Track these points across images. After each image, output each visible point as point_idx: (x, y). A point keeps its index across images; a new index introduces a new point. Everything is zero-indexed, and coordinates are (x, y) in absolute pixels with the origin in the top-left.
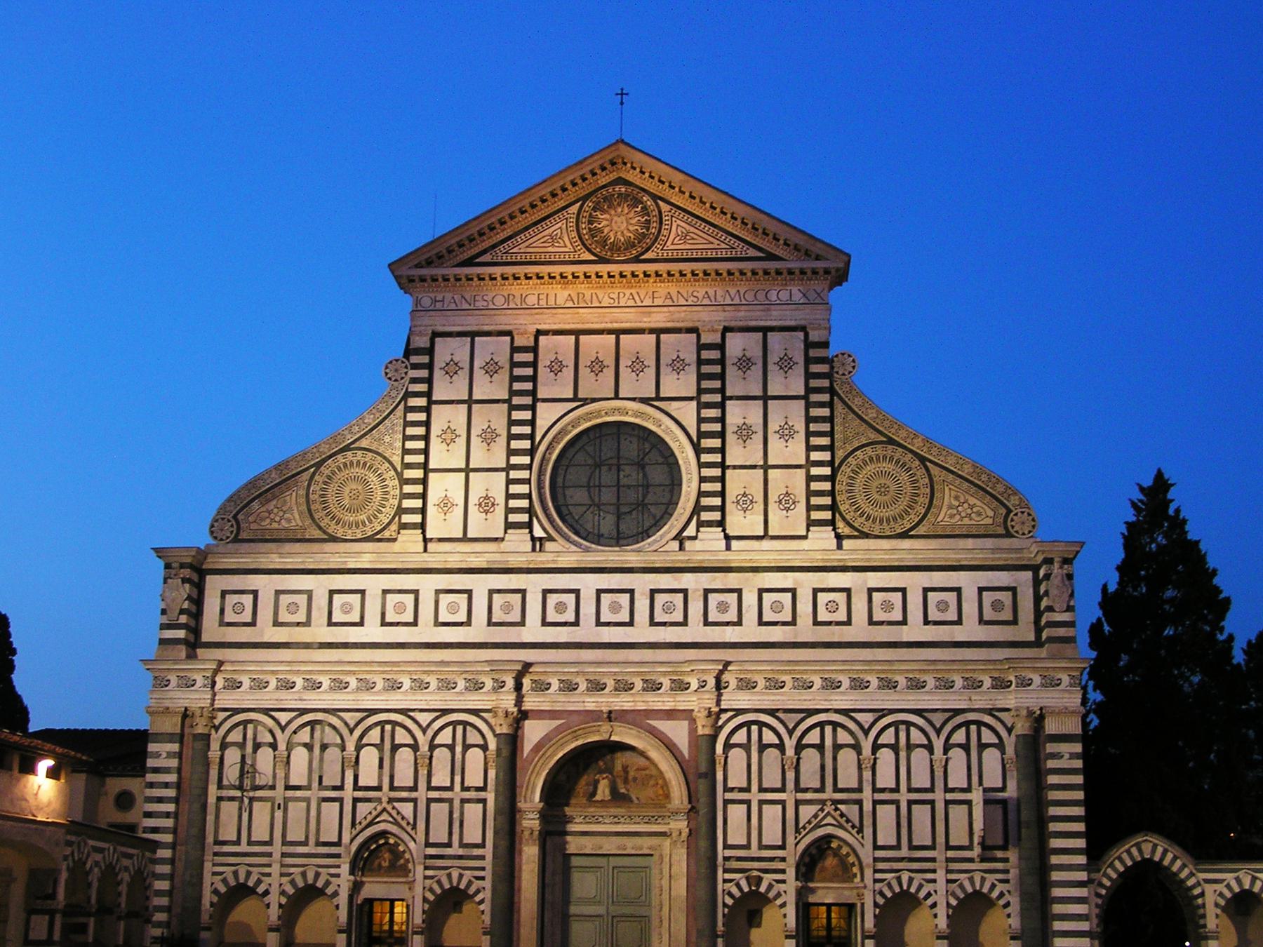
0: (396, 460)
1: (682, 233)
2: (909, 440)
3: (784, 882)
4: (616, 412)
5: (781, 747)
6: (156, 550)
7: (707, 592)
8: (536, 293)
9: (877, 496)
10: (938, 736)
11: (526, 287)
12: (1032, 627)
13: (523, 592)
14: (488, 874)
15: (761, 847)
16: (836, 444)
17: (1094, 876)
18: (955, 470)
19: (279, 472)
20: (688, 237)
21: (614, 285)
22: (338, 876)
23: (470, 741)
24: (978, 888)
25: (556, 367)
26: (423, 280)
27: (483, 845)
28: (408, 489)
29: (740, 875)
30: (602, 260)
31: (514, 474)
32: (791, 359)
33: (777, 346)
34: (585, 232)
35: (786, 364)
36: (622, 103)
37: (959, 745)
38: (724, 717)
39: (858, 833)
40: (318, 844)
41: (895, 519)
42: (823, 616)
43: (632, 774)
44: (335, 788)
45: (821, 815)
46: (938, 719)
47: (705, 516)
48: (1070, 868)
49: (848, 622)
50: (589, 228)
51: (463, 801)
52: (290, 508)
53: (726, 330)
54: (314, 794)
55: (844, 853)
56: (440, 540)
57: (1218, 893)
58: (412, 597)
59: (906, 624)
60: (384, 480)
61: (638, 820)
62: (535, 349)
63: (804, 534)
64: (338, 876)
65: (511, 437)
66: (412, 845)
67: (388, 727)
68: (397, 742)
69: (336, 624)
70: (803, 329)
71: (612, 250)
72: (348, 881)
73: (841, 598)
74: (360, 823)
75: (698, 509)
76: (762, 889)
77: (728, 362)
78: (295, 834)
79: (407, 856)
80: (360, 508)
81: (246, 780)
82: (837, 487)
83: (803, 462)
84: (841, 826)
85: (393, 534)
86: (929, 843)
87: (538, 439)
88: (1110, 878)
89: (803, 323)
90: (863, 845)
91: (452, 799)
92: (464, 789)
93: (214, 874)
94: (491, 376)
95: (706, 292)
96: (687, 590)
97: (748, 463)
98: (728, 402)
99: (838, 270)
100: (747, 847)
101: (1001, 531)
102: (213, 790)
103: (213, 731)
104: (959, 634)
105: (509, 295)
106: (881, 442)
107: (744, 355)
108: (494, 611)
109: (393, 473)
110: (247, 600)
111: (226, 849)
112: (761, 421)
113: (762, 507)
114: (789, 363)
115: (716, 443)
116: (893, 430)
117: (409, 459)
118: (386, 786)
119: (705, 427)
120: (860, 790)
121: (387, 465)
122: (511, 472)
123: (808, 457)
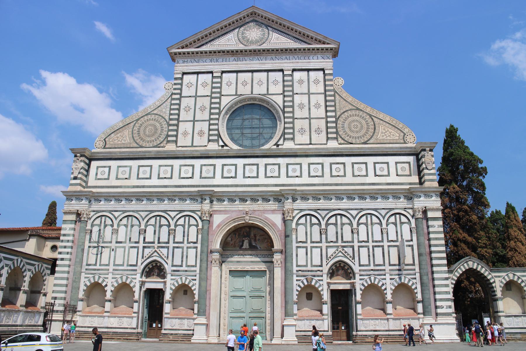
0: (167, 118)
3: (322, 280)
4: (252, 100)
5: (320, 224)
7: (288, 165)
8: (222, 58)
10: (384, 220)
13: (214, 166)
14: (197, 278)
15: (312, 266)
16: (337, 110)
17: (451, 275)
22: (135, 279)
23: (191, 223)
24: (403, 282)
25: (229, 84)
26: (180, 54)
27: (196, 266)
28: (171, 128)
29: (304, 278)
31: (212, 122)
34: (240, 37)
37: (393, 223)
38: (296, 212)
39: (352, 259)
40: (128, 265)
42: (334, 173)
43: (258, 238)
44: (136, 243)
45: (337, 252)
46: (383, 212)
47: (286, 136)
48: (441, 272)
49: (345, 176)
51: (188, 248)
52: (126, 136)
53: (294, 70)
54: (128, 245)
55: (346, 268)
57: (500, 281)
60: (162, 125)
61: (260, 256)
64: (135, 279)
65: (211, 108)
66: (166, 266)
67: (158, 218)
68: (162, 224)
69: (140, 179)
70: (323, 70)
71: (251, 43)
72: (140, 281)
73: (341, 166)
74: (146, 257)
75: (284, 134)
76: (313, 284)
77: (295, 81)
78: (119, 261)
79: (164, 271)
80: (153, 135)
81: (100, 239)
82: (338, 126)
83: (324, 116)
84: (346, 257)
85: (164, 145)
86: (382, 263)
88: (456, 276)
89: (323, 67)
90: (355, 264)
91: (184, 247)
92: (188, 243)
93: (85, 278)
98: (295, 96)
100: (306, 266)
101: (402, 141)
102: (87, 244)
103: (89, 220)
104: (389, 180)
106: (354, 109)
109: (165, 122)
110: (107, 170)
111: (91, 267)
112: (308, 102)
113: (309, 133)
115: (290, 109)
116: (358, 105)
117: (171, 117)
118: (156, 242)
119: (286, 104)
120: (353, 242)
121: (163, 120)
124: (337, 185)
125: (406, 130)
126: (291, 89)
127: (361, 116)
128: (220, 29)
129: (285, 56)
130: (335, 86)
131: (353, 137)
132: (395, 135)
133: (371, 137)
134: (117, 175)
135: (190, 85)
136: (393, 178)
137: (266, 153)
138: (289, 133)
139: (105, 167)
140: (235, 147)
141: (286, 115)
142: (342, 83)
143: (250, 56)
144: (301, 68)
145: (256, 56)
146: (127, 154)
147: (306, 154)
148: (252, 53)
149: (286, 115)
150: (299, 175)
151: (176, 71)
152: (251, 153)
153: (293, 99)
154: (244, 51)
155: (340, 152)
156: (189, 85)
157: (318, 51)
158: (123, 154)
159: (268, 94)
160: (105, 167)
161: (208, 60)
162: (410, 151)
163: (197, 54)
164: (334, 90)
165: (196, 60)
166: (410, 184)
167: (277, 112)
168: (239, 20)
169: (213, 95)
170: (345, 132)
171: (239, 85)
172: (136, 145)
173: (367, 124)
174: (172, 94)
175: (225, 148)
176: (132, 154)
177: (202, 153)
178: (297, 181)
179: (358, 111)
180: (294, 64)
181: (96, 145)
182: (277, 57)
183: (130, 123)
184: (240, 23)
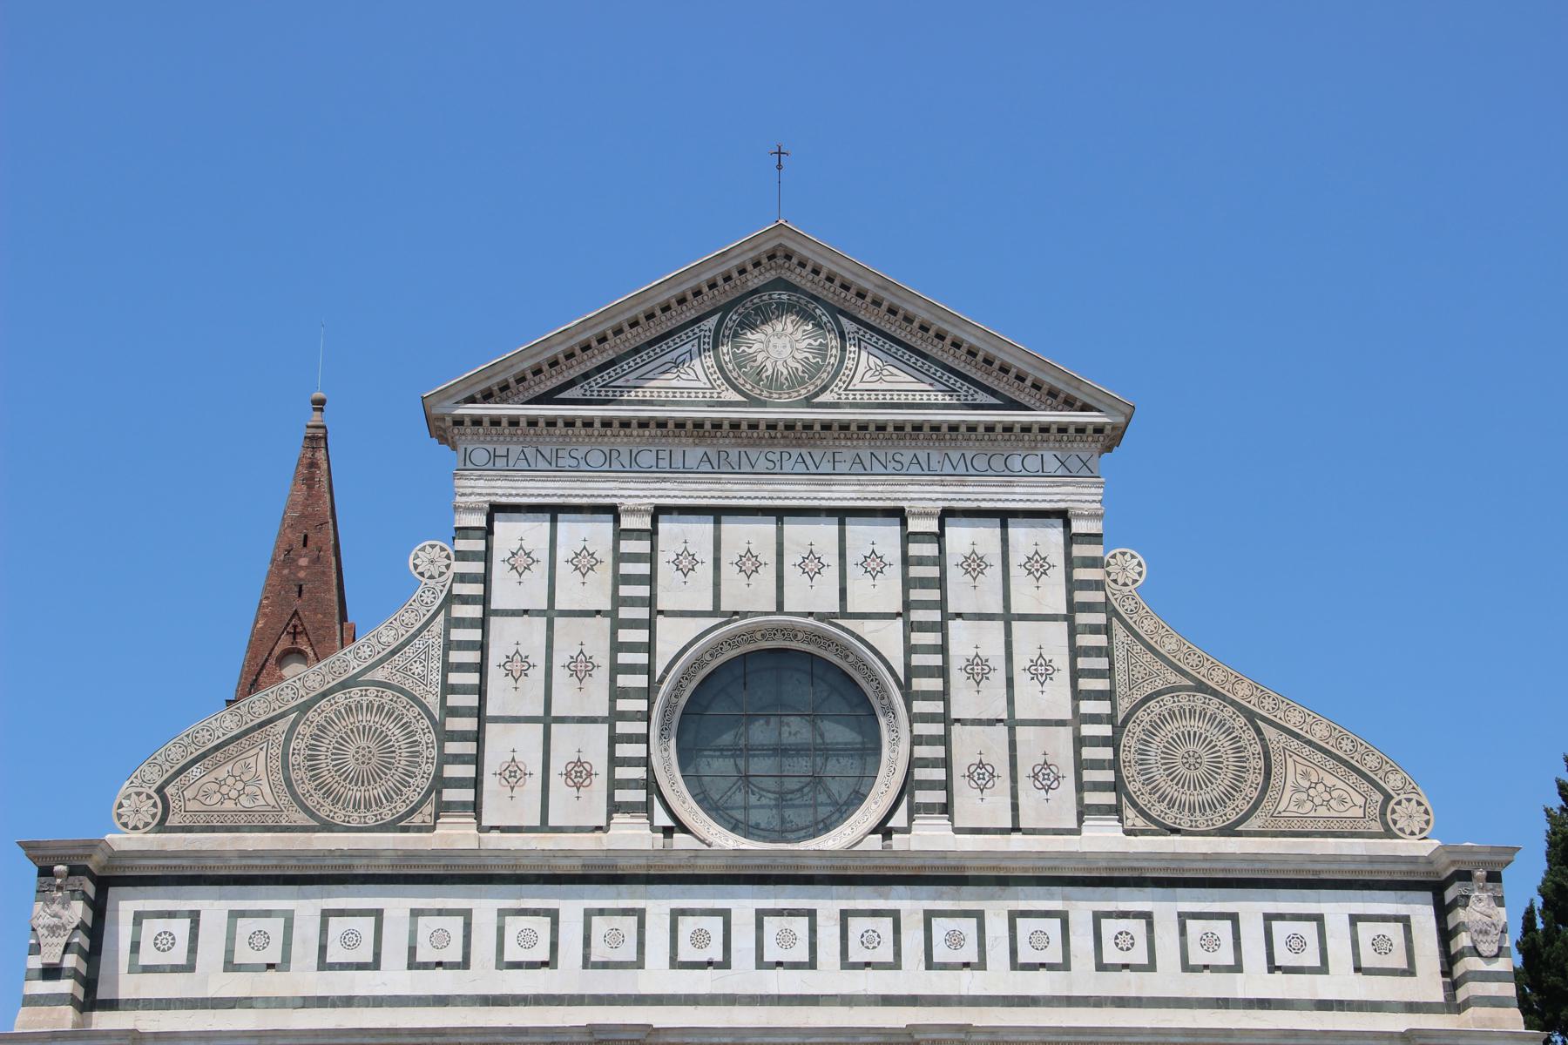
0: (433, 702)
1: (876, 364)
2: (1228, 686)
4: (779, 634)
6: (25, 846)
8: (654, 449)
9: (1183, 770)
11: (638, 440)
12: (1440, 979)
16: (1118, 690)
18: (1300, 732)
19: (236, 718)
20: (885, 372)
21: (776, 441)
25: (684, 562)
26: (477, 421)
28: (452, 748)
30: (753, 402)
31: (622, 727)
34: (727, 359)
35: (1037, 566)
36: (779, 167)
41: (1212, 806)
42: (1111, 955)
47: (922, 797)
49: (1151, 966)
50: (734, 353)
52: (256, 778)
59: (1242, 972)
60: (411, 734)
63: (1073, 825)
65: (616, 669)
70: (1063, 516)
73: (1137, 927)
77: (950, 562)
82: (1122, 756)
83: (1068, 715)
85: (428, 819)
87: (659, 673)
89: (1062, 505)
94: (584, 575)
95: (915, 455)
96: (899, 911)
97: (984, 716)
98: (951, 623)
99: (1114, 428)
104: (1324, 988)
105: (611, 450)
109: (427, 722)
110: (181, 927)
112: (1002, 652)
113: (1007, 784)
114: (1042, 566)
115: (935, 684)
117: (454, 700)
119: (917, 660)
121: (417, 709)
123: (1076, 709)
124: (1121, 1002)
125: (1393, 782)
126: (934, 595)
127: (1213, 718)
128: (642, 320)
129: (912, 453)
130: (1111, 587)
131: (1182, 805)
132: (1348, 800)
133: (1255, 807)
134: (230, 952)
135: (521, 561)
136: (1341, 983)
137: (845, 868)
138: (931, 785)
139: (171, 915)
142: (1140, 574)
143: (770, 446)
144: (974, 505)
145: (794, 446)
146: (274, 862)
147: (1002, 874)
148: (779, 435)
149: (919, 707)
150: (974, 959)
151: (464, 499)
152: (785, 867)
153: (945, 638)
154: (744, 426)
155: (1132, 869)
156: (521, 561)
157: (1045, 435)
158: (258, 862)
159: (844, 614)
160: (171, 915)
161: (596, 459)
162: (1411, 872)
163: (551, 429)
164: (1107, 607)
166: (1412, 1007)
167: (881, 689)
168: (720, 282)
170: (1149, 781)
171: (728, 571)
172: (301, 818)
173: (1238, 750)
174: (451, 599)
175: (680, 841)
176: (293, 862)
177: (587, 862)
178: (968, 983)
179: (1200, 695)
181: (119, 816)
182: (881, 455)
183: (270, 721)
184: (725, 291)
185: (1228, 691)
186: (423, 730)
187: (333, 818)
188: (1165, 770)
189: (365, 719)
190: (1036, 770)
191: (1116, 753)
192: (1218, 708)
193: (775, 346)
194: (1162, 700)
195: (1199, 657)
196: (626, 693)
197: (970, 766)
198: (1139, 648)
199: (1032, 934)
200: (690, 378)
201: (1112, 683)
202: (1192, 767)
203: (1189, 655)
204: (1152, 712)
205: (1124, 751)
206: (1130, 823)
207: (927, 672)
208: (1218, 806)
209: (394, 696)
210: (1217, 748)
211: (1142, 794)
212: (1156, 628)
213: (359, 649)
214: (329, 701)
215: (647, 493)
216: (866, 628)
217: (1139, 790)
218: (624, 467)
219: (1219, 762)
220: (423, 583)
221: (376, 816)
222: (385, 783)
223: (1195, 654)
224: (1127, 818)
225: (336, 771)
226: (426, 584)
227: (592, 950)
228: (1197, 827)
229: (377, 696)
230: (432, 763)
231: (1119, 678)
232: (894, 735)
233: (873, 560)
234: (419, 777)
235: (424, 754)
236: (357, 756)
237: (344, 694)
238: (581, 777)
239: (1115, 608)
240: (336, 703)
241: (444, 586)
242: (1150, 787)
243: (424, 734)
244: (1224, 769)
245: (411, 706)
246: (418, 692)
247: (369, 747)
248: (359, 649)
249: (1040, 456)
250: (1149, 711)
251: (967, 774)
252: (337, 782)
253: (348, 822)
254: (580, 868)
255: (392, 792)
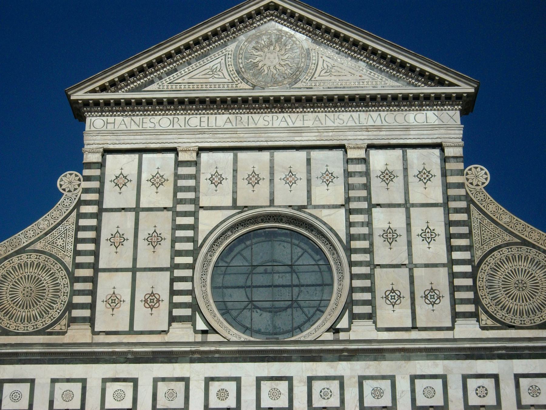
0: (68, 261)
7: (362, 379)
13: (186, 380)
26: (97, 103)
28: (78, 286)
31: (178, 273)
32: (429, 172)
33: (415, 161)
34: (241, 66)
35: (425, 176)
41: (534, 312)
47: (357, 310)
56: (108, 333)
58: (79, 385)
60: (56, 279)
62: (196, 163)
63: (449, 325)
65: (174, 240)
70: (439, 146)
75: (350, 303)
77: (373, 175)
80: (34, 304)
82: (478, 284)
83: (445, 261)
85: (63, 327)
87: (200, 242)
89: (439, 141)
94: (157, 188)
97: (394, 263)
98: (374, 210)
107: (387, 169)
108: (159, 398)
109: (64, 272)
112: (404, 225)
114: (427, 176)
115: (365, 244)
117: (80, 259)
121: (59, 265)
122: (176, 271)
135: (121, 181)
140: (235, 335)
141: (355, 257)
142: (486, 179)
149: (355, 257)
164: (467, 198)
165: (137, 119)
169: (180, 208)
171: (242, 184)
175: (211, 337)
179: (524, 248)
180: (370, 133)
185: (541, 244)
186: (62, 277)
187: (9, 327)
188: (504, 291)
189: (30, 271)
190: (426, 293)
191: (475, 282)
192: (535, 255)
193: (269, 58)
194: (502, 251)
195: (523, 225)
196: (180, 253)
197: (386, 291)
198: (487, 221)
199: (425, 389)
200: (220, 77)
201: (471, 241)
202: (521, 289)
203: (517, 224)
204: (496, 258)
205: (479, 281)
206: (484, 322)
207: (359, 237)
208: (537, 311)
209: (46, 258)
210: (535, 278)
211: (491, 305)
212: (496, 209)
213: (27, 232)
214: (9, 261)
215: (194, 140)
216: (324, 214)
217: (489, 303)
218: (181, 127)
219: (537, 286)
220: (64, 195)
221: (33, 326)
222: (39, 308)
223: (520, 224)
224: (482, 320)
225: (12, 301)
226: (66, 195)
227: (158, 401)
228: (524, 324)
229: (36, 258)
230: (67, 296)
231: (475, 238)
232: (340, 275)
233: (327, 175)
234: (59, 304)
235: (62, 290)
236: (24, 292)
237: (18, 257)
238: (153, 302)
239: (471, 198)
240: (13, 262)
241: (76, 196)
242: (496, 301)
243: (63, 279)
244: (540, 290)
245: (56, 264)
246: (60, 256)
247: (31, 287)
248: (27, 232)
249: (425, 114)
250: (493, 257)
251: (384, 296)
252: (12, 307)
253: (18, 330)
254: (151, 354)
255: (43, 313)
